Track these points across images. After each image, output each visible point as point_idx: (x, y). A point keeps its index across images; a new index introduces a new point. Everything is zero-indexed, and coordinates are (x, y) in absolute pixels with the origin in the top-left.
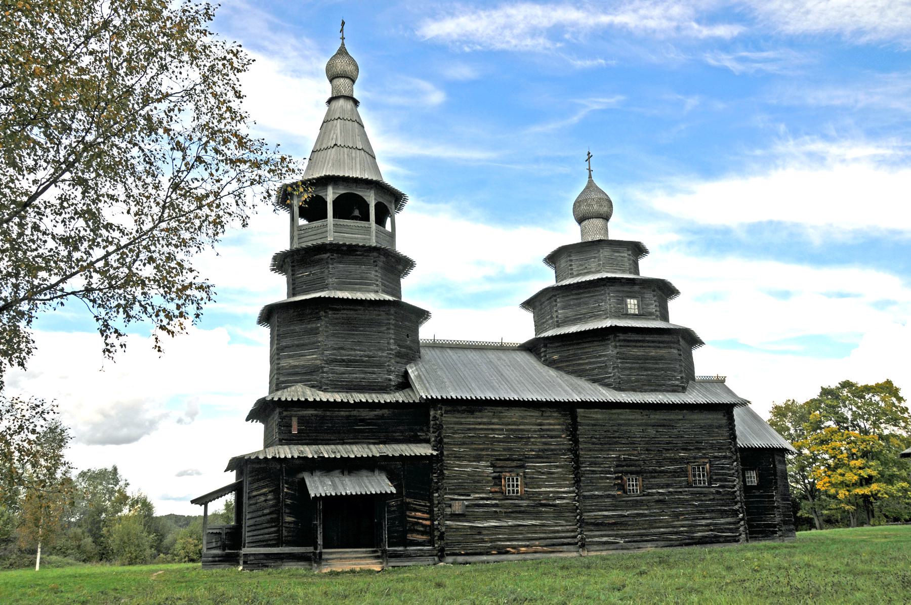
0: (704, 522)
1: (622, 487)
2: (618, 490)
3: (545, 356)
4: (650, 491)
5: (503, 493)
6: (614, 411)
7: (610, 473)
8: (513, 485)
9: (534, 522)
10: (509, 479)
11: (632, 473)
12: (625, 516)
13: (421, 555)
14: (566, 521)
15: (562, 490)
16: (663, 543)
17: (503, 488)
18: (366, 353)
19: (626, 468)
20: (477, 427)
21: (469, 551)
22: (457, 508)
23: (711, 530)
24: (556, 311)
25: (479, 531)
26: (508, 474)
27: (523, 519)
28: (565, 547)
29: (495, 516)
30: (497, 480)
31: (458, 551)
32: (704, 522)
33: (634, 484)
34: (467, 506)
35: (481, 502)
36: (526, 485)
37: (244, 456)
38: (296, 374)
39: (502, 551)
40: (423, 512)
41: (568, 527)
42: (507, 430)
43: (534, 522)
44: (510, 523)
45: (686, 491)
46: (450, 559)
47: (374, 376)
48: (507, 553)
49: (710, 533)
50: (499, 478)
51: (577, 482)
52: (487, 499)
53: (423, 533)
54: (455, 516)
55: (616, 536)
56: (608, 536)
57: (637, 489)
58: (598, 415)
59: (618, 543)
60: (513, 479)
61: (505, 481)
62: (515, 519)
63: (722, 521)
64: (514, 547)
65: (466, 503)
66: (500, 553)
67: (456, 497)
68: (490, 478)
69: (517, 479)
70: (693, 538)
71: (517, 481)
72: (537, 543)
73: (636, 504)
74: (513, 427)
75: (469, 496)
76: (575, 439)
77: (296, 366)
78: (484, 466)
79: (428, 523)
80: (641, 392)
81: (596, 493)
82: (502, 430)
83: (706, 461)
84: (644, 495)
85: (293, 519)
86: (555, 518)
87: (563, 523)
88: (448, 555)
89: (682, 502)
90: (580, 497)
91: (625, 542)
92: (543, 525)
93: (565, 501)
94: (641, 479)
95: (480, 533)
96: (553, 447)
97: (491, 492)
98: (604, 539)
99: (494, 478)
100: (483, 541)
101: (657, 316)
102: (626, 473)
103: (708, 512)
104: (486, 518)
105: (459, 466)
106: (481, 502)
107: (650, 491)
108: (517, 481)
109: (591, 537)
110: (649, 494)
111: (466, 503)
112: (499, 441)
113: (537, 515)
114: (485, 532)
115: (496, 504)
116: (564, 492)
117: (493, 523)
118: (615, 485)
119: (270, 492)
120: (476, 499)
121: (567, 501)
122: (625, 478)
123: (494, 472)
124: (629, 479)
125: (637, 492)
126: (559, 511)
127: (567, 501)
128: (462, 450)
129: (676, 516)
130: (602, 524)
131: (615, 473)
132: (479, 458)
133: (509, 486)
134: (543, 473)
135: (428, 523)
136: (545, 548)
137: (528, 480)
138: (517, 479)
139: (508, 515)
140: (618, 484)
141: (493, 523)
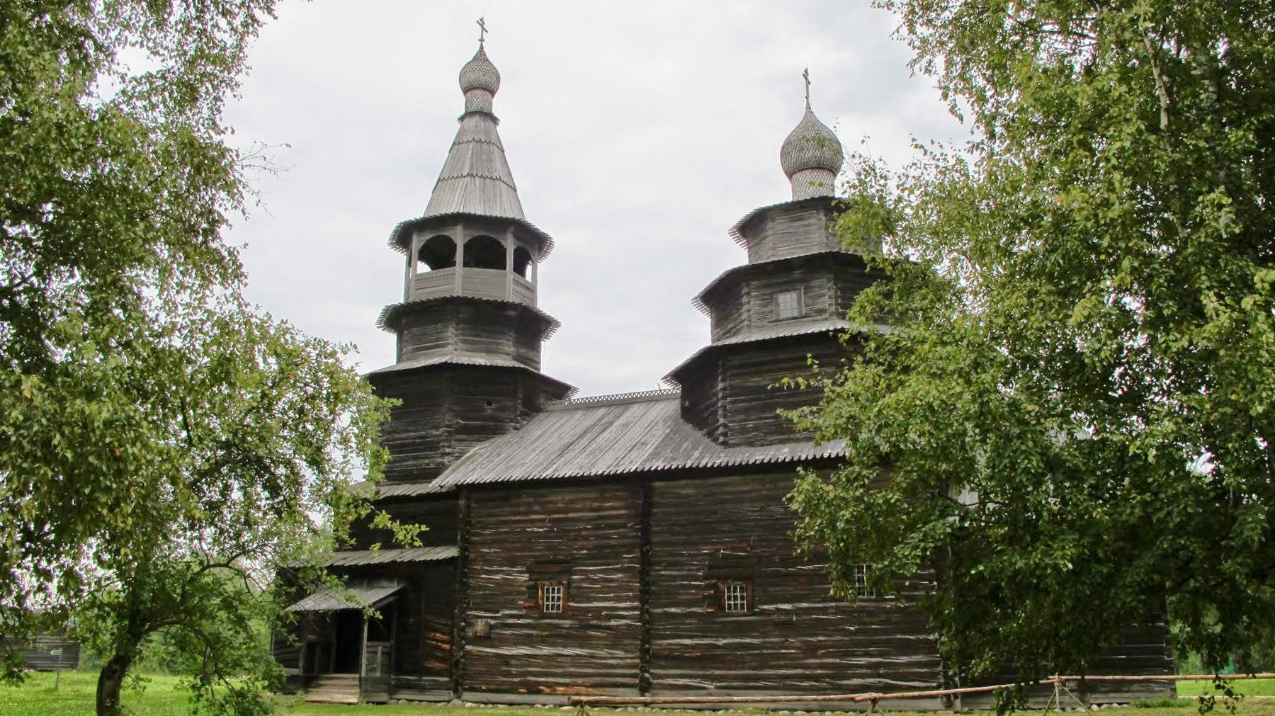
0: (864, 660)
1: (717, 601)
2: (709, 606)
4: (765, 607)
6: (711, 481)
7: (696, 578)
8: (553, 598)
10: (548, 589)
11: (735, 579)
13: (437, 686)
14: (626, 651)
15: (621, 605)
17: (540, 602)
19: (721, 571)
20: (513, 518)
21: (491, 687)
22: (480, 626)
23: (880, 676)
25: (505, 660)
26: (547, 583)
27: (565, 646)
28: (621, 690)
29: (528, 641)
30: (533, 590)
31: (477, 686)
32: (864, 660)
33: (735, 597)
34: (491, 627)
36: (569, 597)
39: (533, 689)
40: (443, 634)
41: (629, 661)
42: (550, 521)
45: (832, 607)
46: (466, 695)
48: (539, 692)
49: (876, 680)
50: (535, 588)
51: (645, 596)
52: (519, 617)
53: (441, 660)
54: (486, 639)
55: (704, 677)
56: (691, 677)
57: (742, 605)
58: (687, 489)
60: (553, 589)
61: (543, 592)
62: (553, 645)
63: (904, 659)
64: (548, 685)
65: (492, 622)
66: (530, 692)
67: (482, 614)
68: (524, 589)
69: (559, 589)
71: (559, 592)
72: (580, 681)
73: (739, 629)
74: (561, 516)
76: (646, 531)
78: (518, 572)
79: (447, 647)
80: (762, 445)
81: (673, 610)
82: (542, 521)
84: (754, 614)
86: (608, 647)
87: (621, 654)
88: (465, 690)
89: (821, 627)
90: (646, 618)
92: (592, 656)
93: (623, 622)
95: (508, 664)
96: (613, 542)
97: (525, 608)
99: (528, 588)
100: (508, 674)
101: (831, 315)
102: (724, 579)
103: (873, 644)
104: (518, 641)
105: (487, 572)
106: (511, 621)
107: (765, 607)
108: (559, 592)
109: (662, 677)
110: (763, 612)
111: (492, 622)
112: (539, 536)
113: (583, 641)
114: (513, 662)
115: (529, 624)
118: (705, 597)
121: (628, 622)
122: (721, 586)
124: (729, 589)
125: (742, 608)
126: (617, 638)
127: (628, 622)
129: (811, 650)
132: (512, 562)
133: (548, 600)
134: (595, 581)
135: (447, 647)
136: (591, 690)
137: (573, 591)
138: (559, 589)
139: (543, 641)
140: (710, 596)
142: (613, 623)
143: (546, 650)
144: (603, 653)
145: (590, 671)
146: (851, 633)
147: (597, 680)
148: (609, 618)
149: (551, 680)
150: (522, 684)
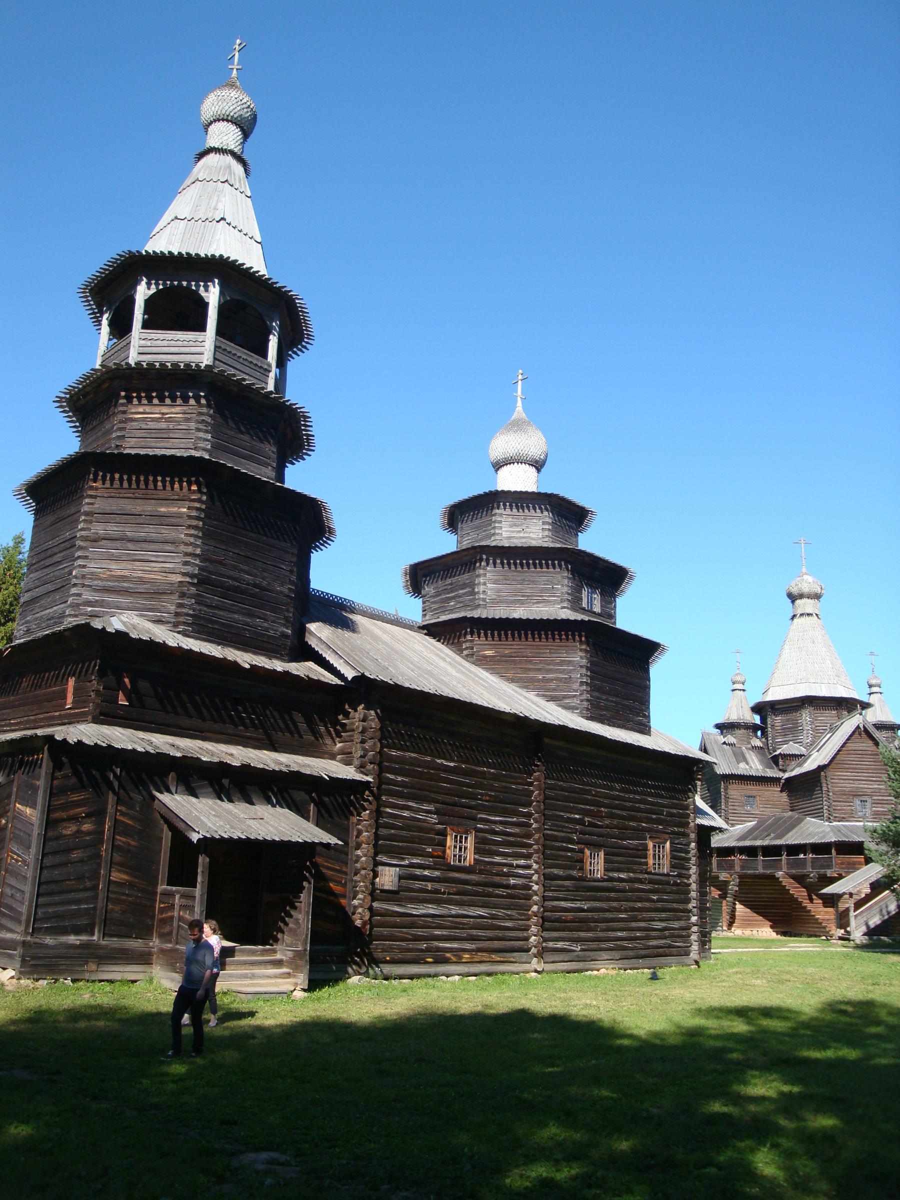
3: (472, 648)
5: (444, 858)
7: (572, 841)
9: (481, 912)
12: (583, 910)
16: (617, 955)
18: (258, 581)
23: (665, 938)
24: (485, 584)
25: (412, 922)
28: (515, 954)
35: (418, 872)
36: (477, 851)
37: (649, 681)
38: (126, 592)
39: (441, 960)
43: (481, 912)
44: (453, 912)
47: (266, 625)
48: (446, 961)
50: (444, 834)
59: (574, 951)
70: (649, 947)
75: (403, 859)
77: (124, 578)
83: (667, 836)
85: (125, 877)
91: (582, 950)
94: (602, 854)
98: (560, 945)
102: (589, 844)
106: (418, 872)
110: (611, 879)
116: (518, 866)
117: (431, 909)
119: (89, 815)
120: (412, 866)
122: (587, 852)
123: (438, 824)
128: (400, 779)
130: (558, 920)
131: (578, 843)
141: (431, 909)
142: (512, 881)
143: (455, 910)
144: (501, 912)
145: (489, 933)
146: (653, 901)
147: (497, 944)
148: (508, 875)
149: (455, 945)
150: (428, 950)
